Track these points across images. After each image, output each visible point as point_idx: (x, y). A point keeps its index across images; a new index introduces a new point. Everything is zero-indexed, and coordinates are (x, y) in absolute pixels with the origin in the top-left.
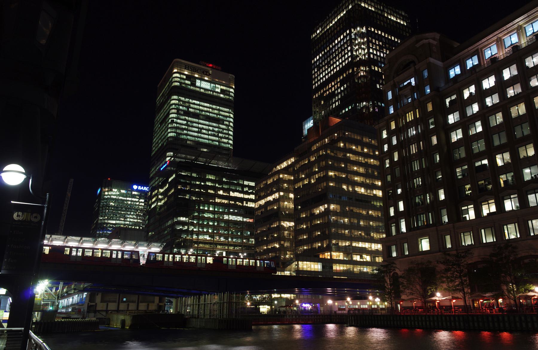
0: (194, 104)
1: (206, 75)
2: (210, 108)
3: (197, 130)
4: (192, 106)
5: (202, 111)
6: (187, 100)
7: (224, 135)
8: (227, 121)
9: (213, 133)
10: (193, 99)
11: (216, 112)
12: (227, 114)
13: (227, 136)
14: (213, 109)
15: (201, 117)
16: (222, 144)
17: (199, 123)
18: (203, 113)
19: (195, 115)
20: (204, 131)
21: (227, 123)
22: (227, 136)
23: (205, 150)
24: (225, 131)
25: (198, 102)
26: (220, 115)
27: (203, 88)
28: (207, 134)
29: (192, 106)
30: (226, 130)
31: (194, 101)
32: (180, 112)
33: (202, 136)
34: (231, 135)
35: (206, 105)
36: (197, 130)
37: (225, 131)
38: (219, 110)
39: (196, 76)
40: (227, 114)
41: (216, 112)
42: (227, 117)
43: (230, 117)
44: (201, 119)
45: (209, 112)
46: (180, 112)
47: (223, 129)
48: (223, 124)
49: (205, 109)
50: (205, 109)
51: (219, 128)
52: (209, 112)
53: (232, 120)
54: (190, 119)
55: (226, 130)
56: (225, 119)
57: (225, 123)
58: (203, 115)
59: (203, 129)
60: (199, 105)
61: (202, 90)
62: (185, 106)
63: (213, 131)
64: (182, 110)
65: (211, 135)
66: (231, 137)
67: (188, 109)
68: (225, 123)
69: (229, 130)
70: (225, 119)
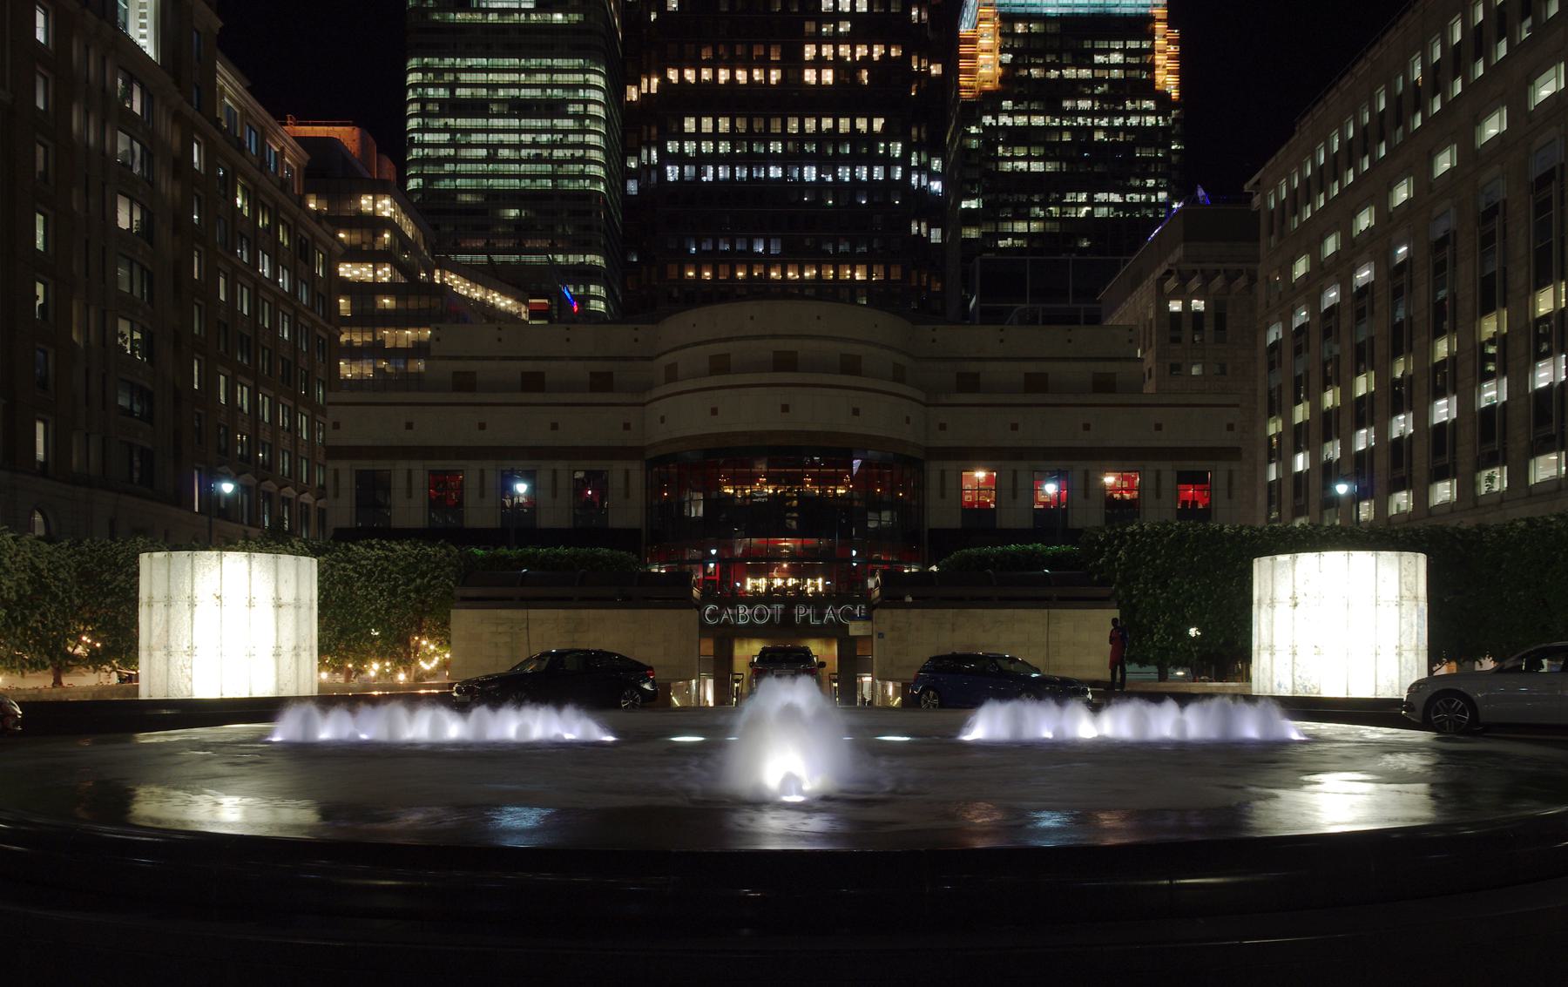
2: (519, 71)
3: (483, 152)
6: (448, 61)
7: (569, 153)
9: (533, 152)
11: (542, 78)
12: (579, 78)
14: (529, 71)
15: (495, 108)
17: (488, 131)
18: (501, 93)
19: (477, 108)
21: (580, 108)
23: (513, 213)
24: (571, 138)
30: (573, 132)
33: (501, 167)
37: (571, 138)
38: (551, 70)
40: (579, 78)
41: (542, 78)
42: (575, 87)
43: (586, 86)
45: (520, 86)
47: (566, 132)
48: (566, 116)
49: (507, 78)
50: (507, 78)
52: (520, 86)
53: (599, 96)
55: (573, 132)
57: (571, 109)
58: (500, 101)
59: (502, 145)
63: (535, 145)
65: (528, 161)
68: (571, 109)
69: (585, 131)
70: (570, 95)
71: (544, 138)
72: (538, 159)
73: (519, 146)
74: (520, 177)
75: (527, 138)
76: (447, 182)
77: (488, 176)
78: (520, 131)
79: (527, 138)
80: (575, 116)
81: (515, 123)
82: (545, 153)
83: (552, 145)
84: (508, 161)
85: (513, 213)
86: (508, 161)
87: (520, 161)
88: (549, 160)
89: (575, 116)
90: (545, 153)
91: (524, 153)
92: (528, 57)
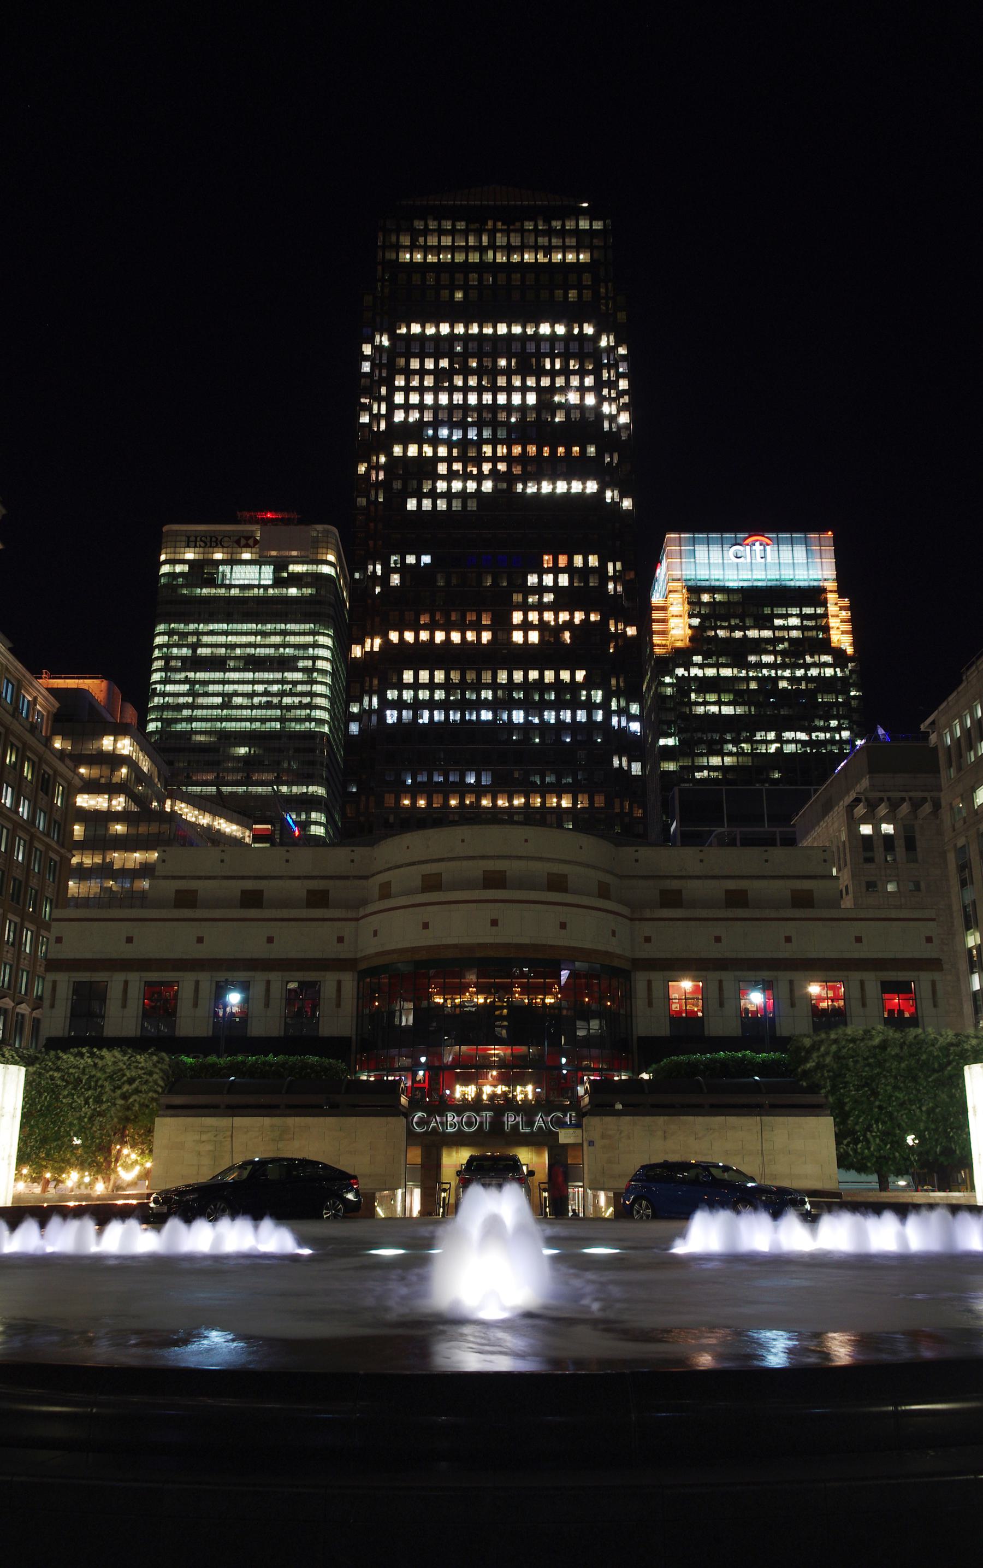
0: (212, 633)
1: (247, 546)
2: (256, 634)
3: (218, 700)
4: (206, 639)
5: (234, 646)
8: (308, 658)
9: (264, 699)
10: (207, 622)
11: (277, 639)
12: (309, 639)
13: (306, 700)
14: (264, 634)
15: (232, 664)
16: (293, 724)
17: (224, 682)
18: (238, 651)
19: (217, 663)
20: (238, 700)
21: (309, 663)
22: (306, 700)
23: (243, 750)
24: (300, 688)
25: (224, 626)
26: (285, 646)
27: (235, 586)
28: (246, 707)
29: (206, 639)
30: (302, 683)
31: (211, 627)
32: (173, 663)
34: (321, 695)
35: (245, 627)
36: (218, 700)
37: (300, 688)
38: (284, 633)
39: (218, 556)
40: (309, 639)
41: (277, 639)
42: (305, 646)
43: (315, 645)
44: (230, 670)
45: (255, 646)
46: (173, 663)
47: (295, 683)
48: (298, 670)
51: (283, 682)
52: (255, 646)
54: (201, 676)
55: (302, 683)
56: (300, 653)
57: (301, 664)
59: (236, 694)
60: (226, 633)
61: (235, 592)
62: (187, 646)
63: (266, 693)
64: (177, 658)
65: (260, 707)
66: (320, 701)
67: (194, 651)
68: (301, 664)
70: (300, 653)
71: (275, 688)
72: (269, 706)
73: (253, 694)
74: (251, 720)
75: (260, 688)
76: (184, 724)
77: (221, 720)
78: (253, 682)
79: (260, 688)
80: (304, 670)
81: (249, 676)
82: (275, 700)
83: (282, 694)
84: (241, 707)
85: (243, 750)
86: (241, 707)
87: (252, 707)
88: (279, 706)
89: (304, 670)
90: (275, 700)
91: (256, 700)
92: (264, 622)
